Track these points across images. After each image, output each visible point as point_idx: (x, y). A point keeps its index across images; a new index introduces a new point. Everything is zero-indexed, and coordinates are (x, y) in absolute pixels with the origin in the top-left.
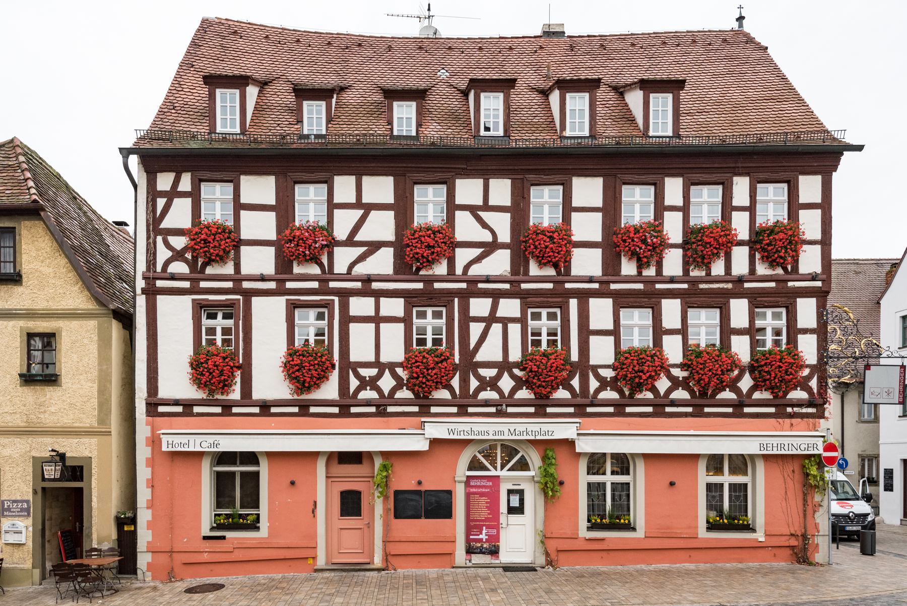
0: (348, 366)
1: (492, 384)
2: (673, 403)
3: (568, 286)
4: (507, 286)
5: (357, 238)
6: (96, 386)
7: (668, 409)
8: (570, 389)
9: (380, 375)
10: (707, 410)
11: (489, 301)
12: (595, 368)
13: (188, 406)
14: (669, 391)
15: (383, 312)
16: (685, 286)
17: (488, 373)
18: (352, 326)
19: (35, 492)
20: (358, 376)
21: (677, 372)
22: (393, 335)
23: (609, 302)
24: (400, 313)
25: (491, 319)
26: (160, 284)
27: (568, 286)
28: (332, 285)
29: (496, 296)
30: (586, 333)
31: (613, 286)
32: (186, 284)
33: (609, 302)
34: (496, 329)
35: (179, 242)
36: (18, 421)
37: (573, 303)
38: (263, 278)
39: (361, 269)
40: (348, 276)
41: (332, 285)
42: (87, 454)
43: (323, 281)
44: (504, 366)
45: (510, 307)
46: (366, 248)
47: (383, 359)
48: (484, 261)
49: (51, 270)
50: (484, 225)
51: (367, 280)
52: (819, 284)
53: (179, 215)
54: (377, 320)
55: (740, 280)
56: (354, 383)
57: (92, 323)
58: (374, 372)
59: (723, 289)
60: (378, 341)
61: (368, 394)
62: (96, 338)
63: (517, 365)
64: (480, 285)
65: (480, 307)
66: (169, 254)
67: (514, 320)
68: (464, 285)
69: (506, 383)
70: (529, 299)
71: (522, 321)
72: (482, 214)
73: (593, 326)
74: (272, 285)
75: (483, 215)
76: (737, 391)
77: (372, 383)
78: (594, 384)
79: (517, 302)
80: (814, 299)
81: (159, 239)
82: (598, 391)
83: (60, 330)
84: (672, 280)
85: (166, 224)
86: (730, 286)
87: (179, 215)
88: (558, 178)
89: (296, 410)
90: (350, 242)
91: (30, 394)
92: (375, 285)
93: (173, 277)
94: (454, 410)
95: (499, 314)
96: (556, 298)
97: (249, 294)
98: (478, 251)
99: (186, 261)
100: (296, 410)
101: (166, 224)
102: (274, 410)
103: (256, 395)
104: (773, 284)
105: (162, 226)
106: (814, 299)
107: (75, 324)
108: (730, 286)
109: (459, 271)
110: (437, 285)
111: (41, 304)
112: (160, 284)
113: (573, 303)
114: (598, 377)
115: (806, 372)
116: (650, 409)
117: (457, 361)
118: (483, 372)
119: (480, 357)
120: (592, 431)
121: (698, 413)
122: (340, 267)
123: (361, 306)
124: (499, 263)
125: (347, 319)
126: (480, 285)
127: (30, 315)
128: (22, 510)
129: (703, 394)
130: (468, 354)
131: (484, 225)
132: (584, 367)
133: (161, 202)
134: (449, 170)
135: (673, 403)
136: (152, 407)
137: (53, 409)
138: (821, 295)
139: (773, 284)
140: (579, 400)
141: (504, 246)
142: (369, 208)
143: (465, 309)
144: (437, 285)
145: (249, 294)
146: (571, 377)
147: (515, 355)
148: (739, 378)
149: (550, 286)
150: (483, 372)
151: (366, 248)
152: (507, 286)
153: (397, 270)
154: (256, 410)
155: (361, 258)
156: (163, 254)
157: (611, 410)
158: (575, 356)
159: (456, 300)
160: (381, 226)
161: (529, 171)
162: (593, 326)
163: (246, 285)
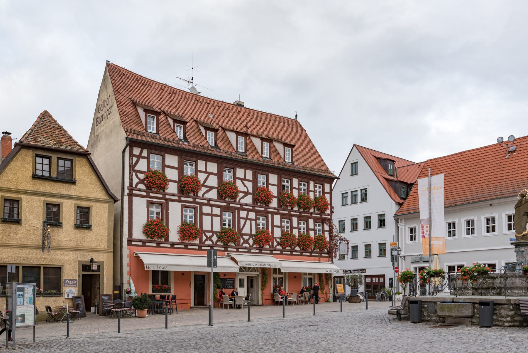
1: (247, 241)
2: (296, 251)
3: (268, 210)
4: (251, 208)
5: (206, 184)
6: (107, 231)
8: (269, 245)
9: (212, 236)
12: (276, 238)
13: (144, 242)
15: (214, 213)
16: (298, 214)
17: (246, 237)
18: (203, 216)
19: (79, 276)
20: (205, 235)
22: (217, 221)
23: (279, 216)
24: (219, 213)
25: (247, 219)
26: (134, 192)
27: (268, 210)
28: (197, 200)
30: (273, 226)
31: (281, 212)
32: (145, 194)
33: (279, 216)
34: (248, 222)
35: (141, 176)
36: (72, 245)
37: (270, 215)
38: (173, 195)
39: (206, 196)
40: (202, 198)
41: (197, 200)
42: (102, 260)
44: (251, 235)
45: (252, 215)
47: (214, 230)
49: (88, 180)
50: (245, 186)
51: (209, 200)
53: (142, 165)
54: (212, 215)
57: (106, 205)
58: (210, 234)
60: (211, 223)
61: (208, 242)
62: (107, 212)
63: (254, 235)
64: (244, 207)
65: (243, 214)
66: (138, 180)
67: (253, 220)
68: (239, 206)
69: (251, 242)
70: (258, 213)
73: (275, 224)
75: (244, 182)
77: (210, 238)
78: (275, 244)
79: (254, 214)
81: (134, 174)
82: (276, 246)
84: (295, 211)
85: (136, 168)
87: (142, 165)
88: (265, 173)
89: (183, 246)
91: (79, 233)
92: (212, 202)
93: (140, 190)
94: (235, 250)
96: (265, 214)
97: (168, 200)
98: (244, 194)
99: (144, 184)
100: (183, 246)
101: (136, 168)
102: (176, 246)
105: (135, 169)
107: (98, 204)
109: (237, 201)
111: (84, 194)
112: (134, 192)
113: (270, 215)
114: (276, 241)
116: (289, 253)
118: (245, 237)
119: (243, 232)
123: (206, 209)
124: (249, 200)
125: (202, 214)
126: (244, 207)
127: (79, 198)
128: (74, 284)
129: (303, 249)
130: (240, 230)
131: (245, 186)
132: (273, 238)
133: (135, 159)
134: (235, 165)
135: (296, 251)
136: (130, 242)
137: (88, 240)
140: (271, 249)
141: (250, 194)
142: (209, 174)
143: (239, 214)
144: (231, 205)
145: (168, 200)
147: (254, 232)
150: (245, 237)
152: (251, 208)
153: (218, 198)
154: (169, 246)
155: (207, 192)
156: (135, 181)
157: (279, 252)
160: (213, 181)
161: (258, 170)
162: (275, 224)
163: (167, 197)
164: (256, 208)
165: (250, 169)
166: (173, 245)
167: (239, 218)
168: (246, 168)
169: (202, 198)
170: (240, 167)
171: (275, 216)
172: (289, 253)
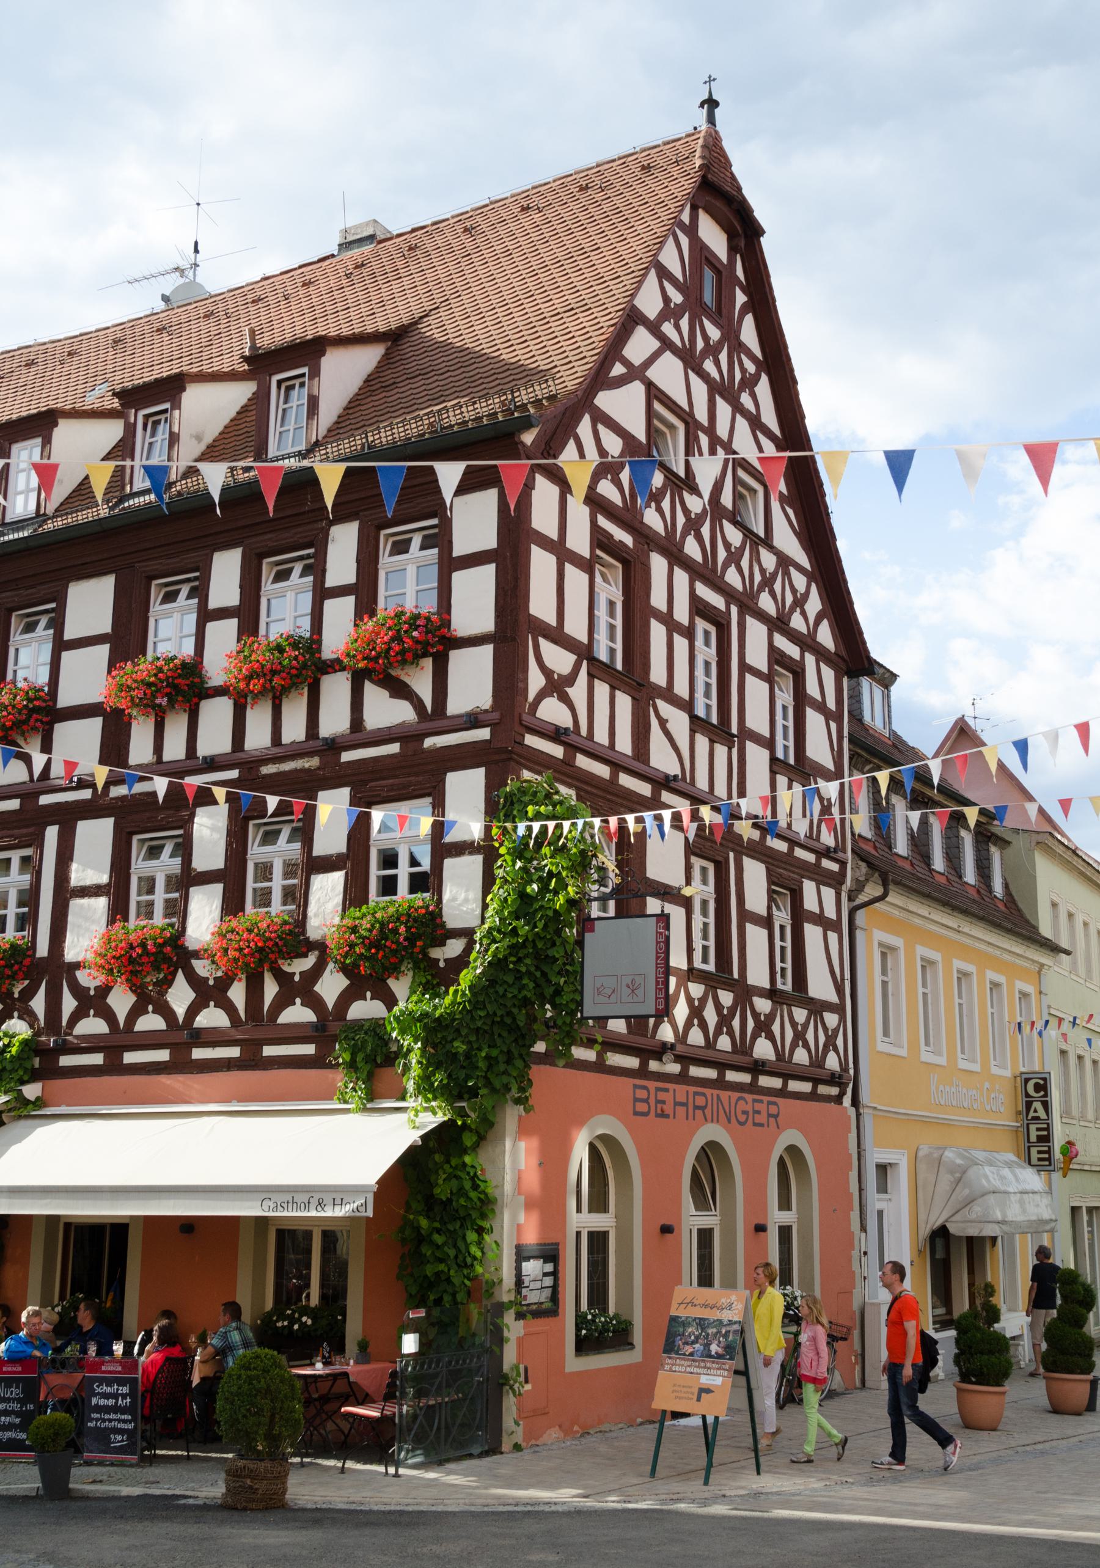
3: (44, 800)
7: (198, 1054)
10: (268, 1051)
14: (193, 1010)
21: (202, 967)
30: (64, 893)
37: (52, 833)
52: (484, 734)
55: (334, 746)
59: (303, 770)
76: (314, 1002)
78: (69, 1003)
80: (482, 771)
82: (75, 1017)
86: (314, 762)
104: (394, 748)
106: (482, 771)
108: (314, 762)
113: (52, 833)
115: (454, 948)
121: (251, 1061)
132: (57, 970)
138: (500, 758)
139: (394, 748)
146: (29, 993)
148: (317, 972)
157: (97, 1059)
158: (42, 949)
171: (84, 828)
172: (163, 1055)
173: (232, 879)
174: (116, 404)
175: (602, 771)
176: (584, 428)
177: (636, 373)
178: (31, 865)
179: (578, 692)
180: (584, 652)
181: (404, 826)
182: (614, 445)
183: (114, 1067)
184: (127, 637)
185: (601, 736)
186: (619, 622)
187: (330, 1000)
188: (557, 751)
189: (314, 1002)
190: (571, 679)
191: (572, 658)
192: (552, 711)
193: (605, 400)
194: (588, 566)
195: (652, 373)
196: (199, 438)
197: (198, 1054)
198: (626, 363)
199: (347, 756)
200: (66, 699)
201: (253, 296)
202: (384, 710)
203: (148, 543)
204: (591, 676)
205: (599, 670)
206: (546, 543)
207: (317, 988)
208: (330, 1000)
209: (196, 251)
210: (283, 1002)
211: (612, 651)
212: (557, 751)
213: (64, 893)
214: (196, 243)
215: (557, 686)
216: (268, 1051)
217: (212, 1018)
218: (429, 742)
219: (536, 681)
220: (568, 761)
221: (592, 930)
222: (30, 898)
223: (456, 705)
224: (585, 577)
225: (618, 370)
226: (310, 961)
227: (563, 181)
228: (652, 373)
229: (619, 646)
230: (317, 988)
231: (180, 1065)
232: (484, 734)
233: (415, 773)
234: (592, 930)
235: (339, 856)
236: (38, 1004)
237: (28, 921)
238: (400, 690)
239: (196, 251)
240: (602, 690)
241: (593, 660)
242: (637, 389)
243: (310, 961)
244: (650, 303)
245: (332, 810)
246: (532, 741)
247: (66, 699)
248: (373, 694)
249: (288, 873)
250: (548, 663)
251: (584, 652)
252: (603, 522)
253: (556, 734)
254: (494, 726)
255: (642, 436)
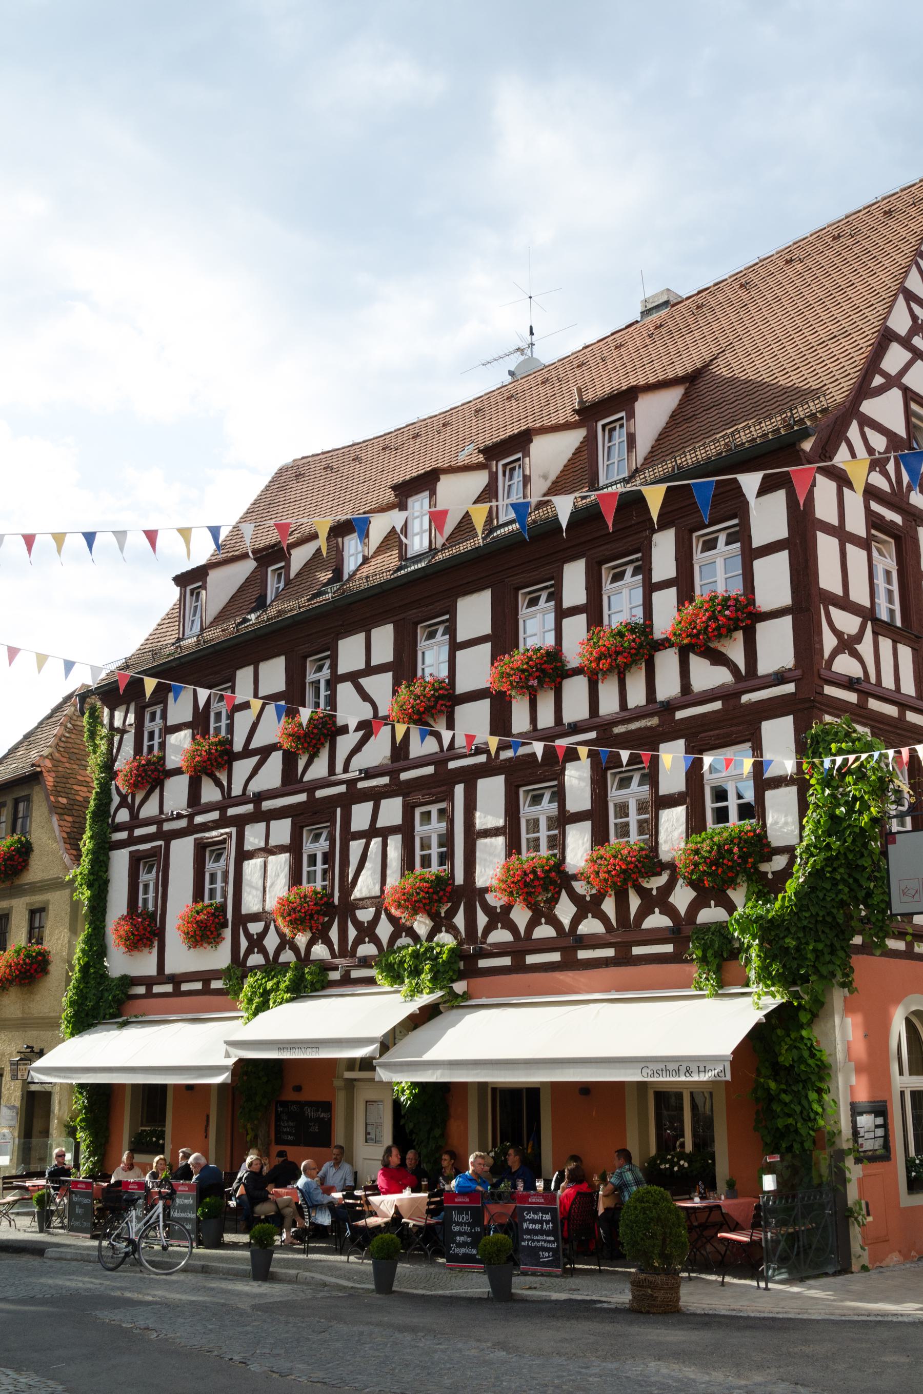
0: (241, 920)
3: (452, 765)
5: (253, 746)
7: (582, 954)
10: (637, 951)
11: (370, 805)
14: (576, 921)
17: (365, 915)
21: (580, 887)
25: (373, 831)
28: (231, 812)
29: (376, 796)
40: (242, 800)
41: (231, 812)
43: (221, 807)
46: (258, 757)
48: (364, 749)
50: (365, 696)
51: (259, 797)
52: (790, 688)
55: (669, 707)
56: (244, 944)
59: (647, 728)
60: (267, 884)
67: (393, 830)
71: (406, 830)
72: (363, 681)
74: (183, 823)
76: (670, 911)
78: (482, 920)
82: (488, 929)
83: (47, 903)
86: (654, 721)
90: (247, 753)
92: (267, 805)
95: (380, 824)
103: (168, 970)
104: (717, 705)
108: (654, 721)
110: (320, 794)
113: (459, 790)
115: (779, 862)
117: (336, 901)
120: (484, 1001)
121: (624, 959)
122: (237, 791)
123: (254, 836)
130: (347, 887)
131: (365, 696)
132: (471, 894)
139: (717, 705)
144: (320, 794)
146: (452, 913)
149: (430, 770)
151: (258, 757)
152: (385, 780)
157: (506, 961)
158: (459, 879)
159: (339, 810)
163: (167, 826)
164: (404, 776)
165: (379, 621)
166: (176, 980)
167: (349, 836)
168: (365, 625)
169: (242, 800)
170: (349, 631)
171: (483, 785)
172: (556, 957)
173: (597, 816)
174: (481, 458)
175: (891, 711)
176: (853, 432)
177: (893, 381)
178: (446, 815)
179: (865, 648)
180: (868, 615)
181: (729, 767)
182: (879, 442)
183: (519, 967)
184: (503, 636)
185: (888, 682)
186: (895, 588)
187: (682, 909)
188: (852, 697)
189: (670, 911)
190: (859, 637)
191: (858, 620)
192: (845, 665)
193: (868, 407)
194: (865, 544)
195: (907, 380)
196: (545, 477)
197: (582, 954)
198: (884, 374)
199: (680, 715)
200: (462, 687)
201: (578, 362)
202: (707, 676)
203: (514, 562)
204: (875, 634)
205: (882, 628)
206: (828, 529)
207: (671, 900)
208: (682, 909)
209: (532, 333)
210: (645, 911)
211: (892, 612)
212: (852, 697)
213: (472, 835)
214: (531, 328)
215: (847, 644)
216: (637, 951)
217: (591, 926)
218: (745, 698)
219: (829, 642)
220: (862, 705)
221: (894, 842)
222: (447, 840)
223: (765, 667)
224: (864, 553)
225: (878, 380)
226: (663, 879)
227: (819, 235)
228: (907, 380)
229: (897, 607)
230: (671, 900)
231: (570, 964)
232: (790, 688)
233: (736, 724)
234: (894, 842)
235: (680, 794)
236: (459, 920)
237: (447, 857)
238: (719, 659)
239: (532, 333)
240: (886, 644)
241: (876, 621)
242: (895, 396)
243: (663, 879)
244: (900, 322)
245: (672, 758)
246: (829, 690)
247: (462, 687)
248: (698, 664)
249: (641, 809)
250: (838, 626)
251: (868, 615)
252: (875, 506)
253: (849, 684)
254: (797, 681)
255: (902, 433)
